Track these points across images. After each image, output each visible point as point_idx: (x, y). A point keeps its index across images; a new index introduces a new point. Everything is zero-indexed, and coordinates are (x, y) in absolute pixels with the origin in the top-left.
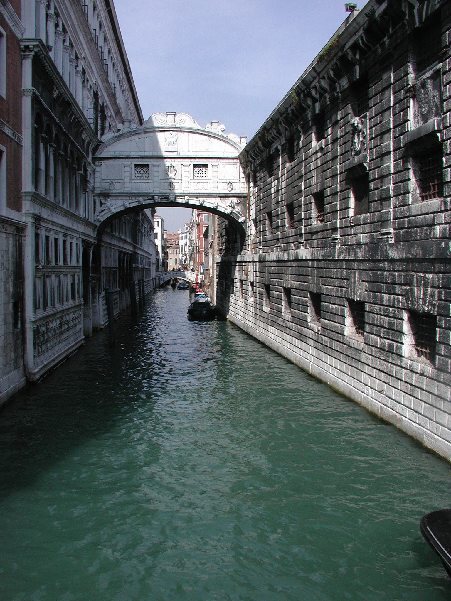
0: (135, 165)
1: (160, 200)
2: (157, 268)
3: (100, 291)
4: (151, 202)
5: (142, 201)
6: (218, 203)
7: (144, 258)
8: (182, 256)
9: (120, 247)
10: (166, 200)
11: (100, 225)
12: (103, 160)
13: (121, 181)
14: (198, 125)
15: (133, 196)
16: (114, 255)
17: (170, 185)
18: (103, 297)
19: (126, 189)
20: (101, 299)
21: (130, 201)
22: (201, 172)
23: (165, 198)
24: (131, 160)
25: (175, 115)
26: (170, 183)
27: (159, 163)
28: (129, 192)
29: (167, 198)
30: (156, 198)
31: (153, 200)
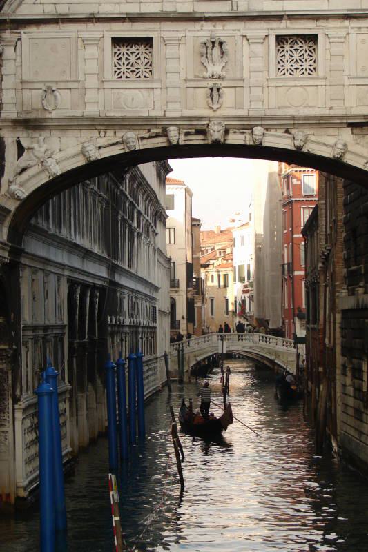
1: (182, 137)
2: (174, 324)
3: (18, 392)
4: (160, 142)
5: (136, 141)
6: (345, 145)
7: (137, 298)
8: (244, 292)
9: (73, 269)
10: (201, 137)
11: (17, 209)
12: (25, 27)
13: (75, 85)
15: (108, 127)
16: (57, 291)
17: (211, 96)
18: (25, 410)
20: (19, 416)
21: (102, 142)
22: (296, 56)
23: (198, 132)
26: (212, 89)
27: (180, 34)
28: (97, 115)
29: (202, 132)
30: (173, 133)
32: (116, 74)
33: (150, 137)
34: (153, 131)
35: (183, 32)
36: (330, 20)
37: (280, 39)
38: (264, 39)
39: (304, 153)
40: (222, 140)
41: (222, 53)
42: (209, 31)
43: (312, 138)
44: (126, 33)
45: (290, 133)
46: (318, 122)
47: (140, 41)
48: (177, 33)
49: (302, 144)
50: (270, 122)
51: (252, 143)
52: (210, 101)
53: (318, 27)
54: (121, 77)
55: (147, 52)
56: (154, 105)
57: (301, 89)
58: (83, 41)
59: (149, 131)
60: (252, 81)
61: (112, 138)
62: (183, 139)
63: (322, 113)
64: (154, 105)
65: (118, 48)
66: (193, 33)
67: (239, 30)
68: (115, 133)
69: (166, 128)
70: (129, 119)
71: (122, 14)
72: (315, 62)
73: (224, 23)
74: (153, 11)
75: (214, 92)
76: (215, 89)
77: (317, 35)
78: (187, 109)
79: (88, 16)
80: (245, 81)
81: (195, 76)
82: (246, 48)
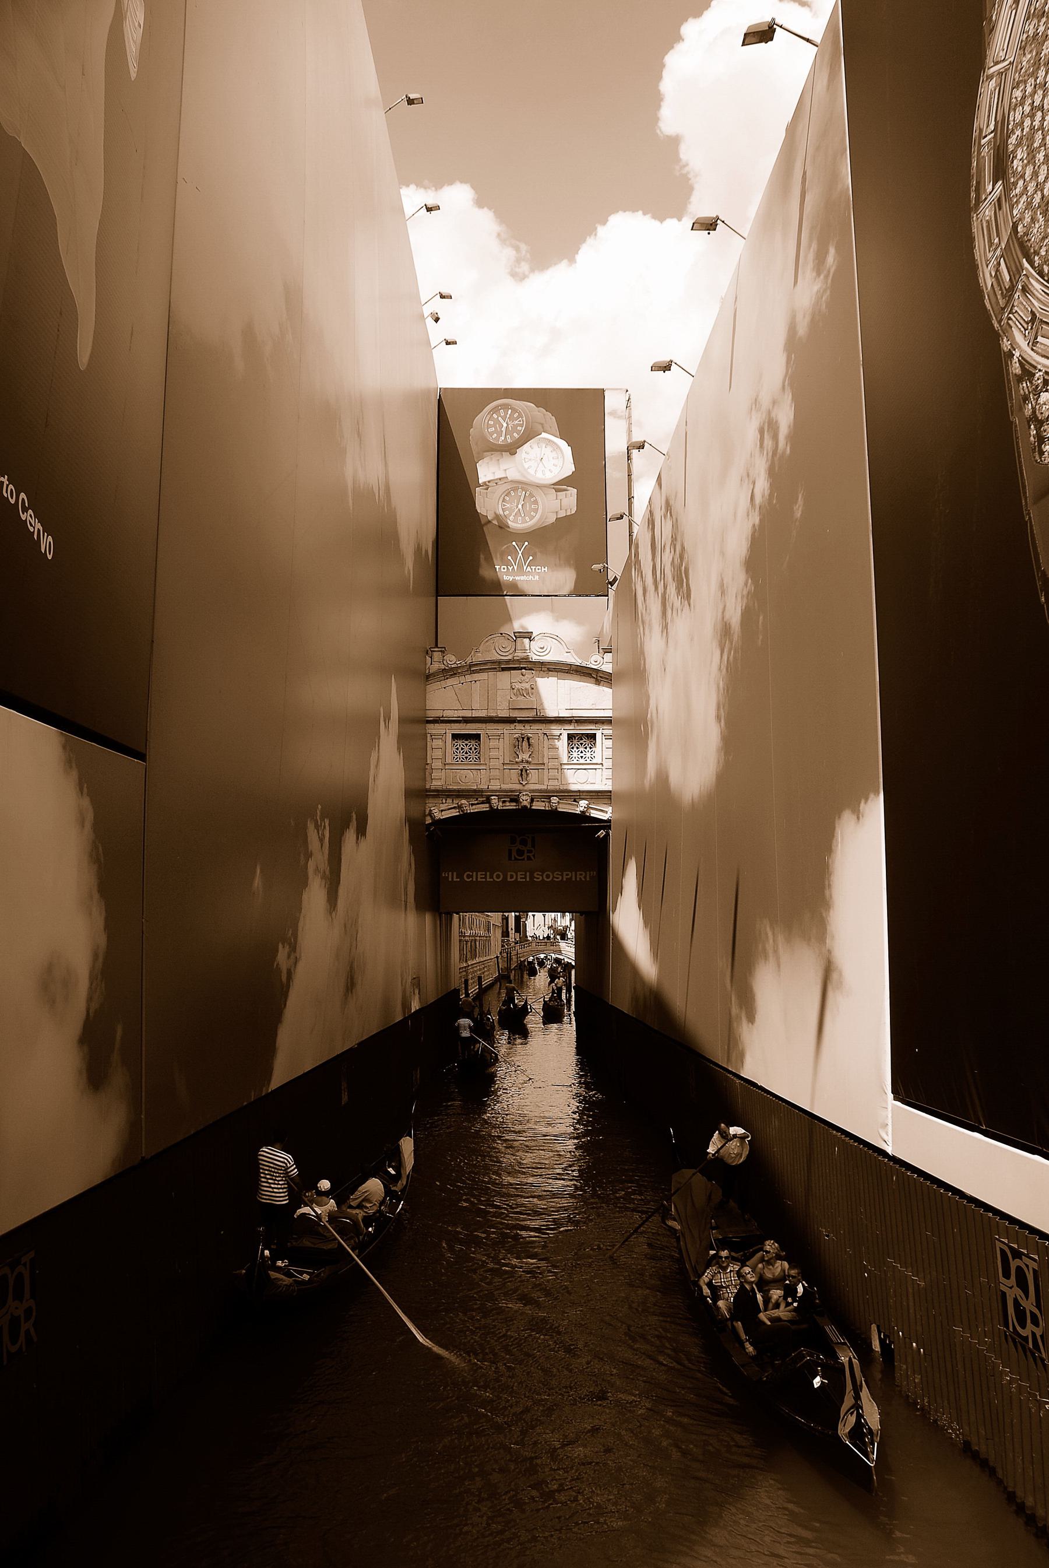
1: (501, 804)
4: (485, 807)
10: (515, 804)
14: (576, 658)
15: (448, 796)
17: (522, 775)
19: (434, 783)
23: (512, 801)
30: (494, 800)
31: (487, 805)
33: (478, 804)
40: (529, 807)
41: (529, 745)
49: (585, 809)
52: (520, 779)
53: (597, 729)
54: (458, 761)
58: (431, 736)
59: (477, 800)
70: (463, 791)
71: (459, 717)
77: (595, 734)
81: (510, 761)
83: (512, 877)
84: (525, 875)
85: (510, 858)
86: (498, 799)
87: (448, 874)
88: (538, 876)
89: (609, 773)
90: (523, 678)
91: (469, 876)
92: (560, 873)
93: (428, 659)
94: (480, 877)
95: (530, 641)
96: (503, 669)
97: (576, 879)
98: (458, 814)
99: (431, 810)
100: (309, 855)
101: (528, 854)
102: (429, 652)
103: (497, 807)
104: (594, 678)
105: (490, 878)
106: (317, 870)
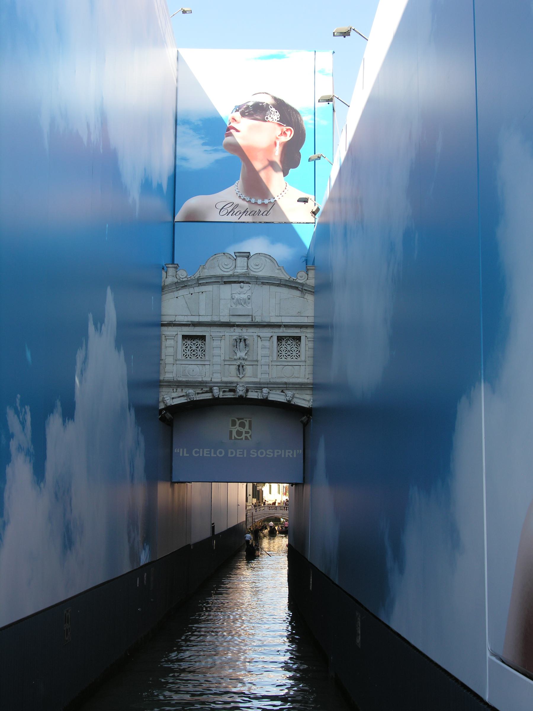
0: (183, 336)
1: (221, 393)
4: (208, 396)
10: (232, 393)
15: (178, 386)
17: (239, 370)
21: (174, 395)
23: (231, 391)
24: (175, 328)
25: (248, 257)
26: (239, 366)
27: (221, 334)
28: (172, 379)
29: (233, 390)
30: (216, 390)
31: (210, 394)
32: (185, 355)
33: (202, 393)
34: (204, 389)
35: (223, 333)
36: (308, 328)
37: (279, 338)
38: (270, 338)
39: (292, 404)
41: (246, 345)
42: (239, 332)
43: (297, 395)
44: (191, 333)
45: (284, 393)
46: (300, 386)
47: (198, 337)
48: (220, 333)
50: (272, 386)
51: (262, 398)
54: (187, 358)
55: (202, 343)
56: (205, 374)
57: (290, 367)
58: (165, 337)
59: (202, 389)
60: (263, 361)
61: (181, 393)
62: (222, 395)
63: (303, 381)
64: (205, 374)
65: (186, 341)
66: (230, 333)
67: (255, 333)
68: (182, 390)
69: (212, 388)
71: (188, 321)
72: (299, 352)
73: (247, 328)
74: (206, 320)
75: (240, 368)
76: (241, 366)
77: (300, 337)
78: (224, 377)
79: (169, 322)
80: (259, 362)
81: (229, 358)
82: (260, 343)
83: (232, 453)
84: (243, 452)
85: (231, 438)
86: (220, 389)
87: (180, 450)
88: (253, 453)
89: (309, 369)
90: (241, 290)
91: (196, 452)
92: (272, 451)
93: (164, 274)
94: (205, 453)
95: (248, 259)
96: (225, 283)
97: (285, 455)
98: (186, 401)
99: (164, 398)
100: (10, 436)
101: (246, 435)
102: (165, 268)
103: (219, 396)
104: (300, 291)
105: (214, 454)
106: (20, 448)
